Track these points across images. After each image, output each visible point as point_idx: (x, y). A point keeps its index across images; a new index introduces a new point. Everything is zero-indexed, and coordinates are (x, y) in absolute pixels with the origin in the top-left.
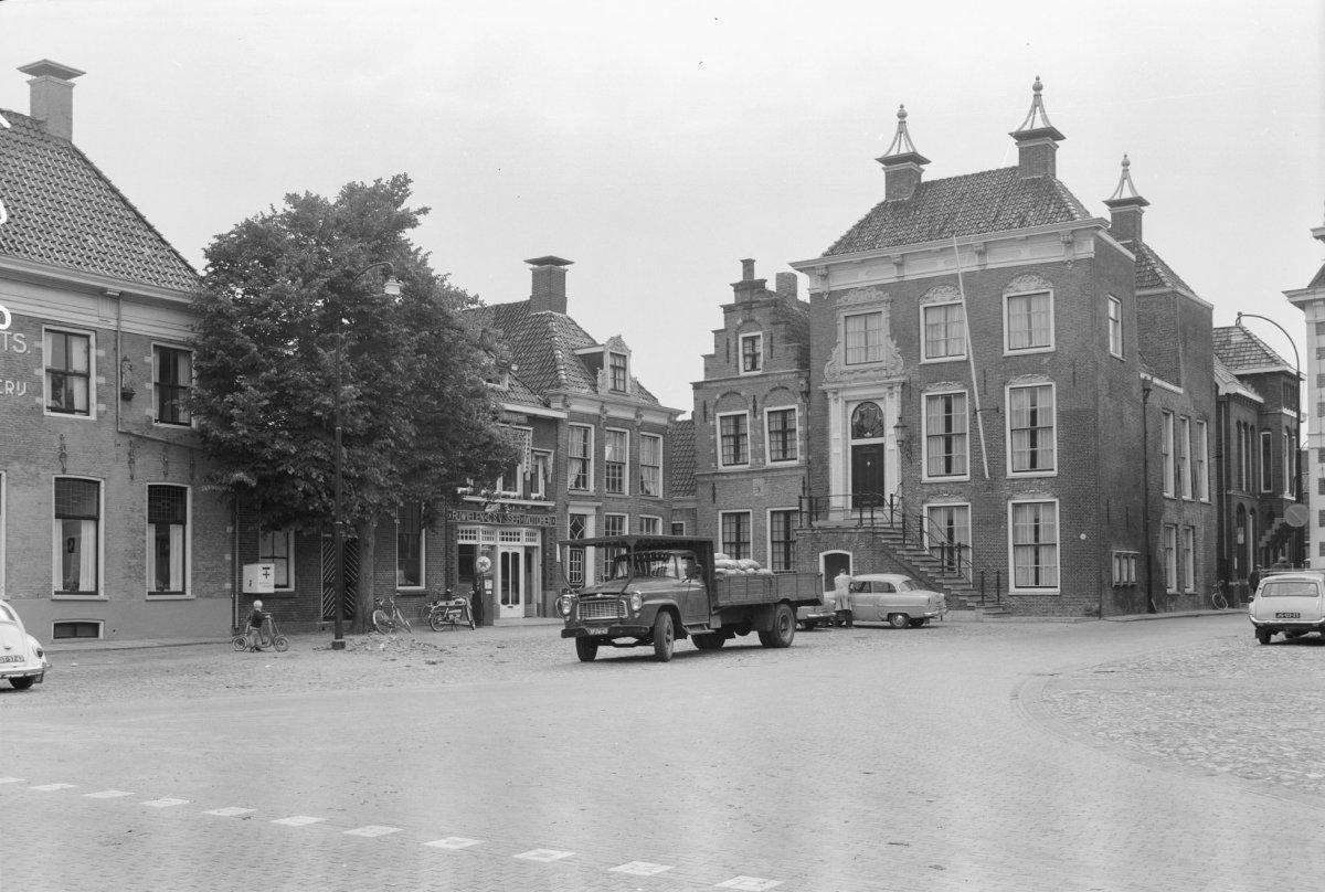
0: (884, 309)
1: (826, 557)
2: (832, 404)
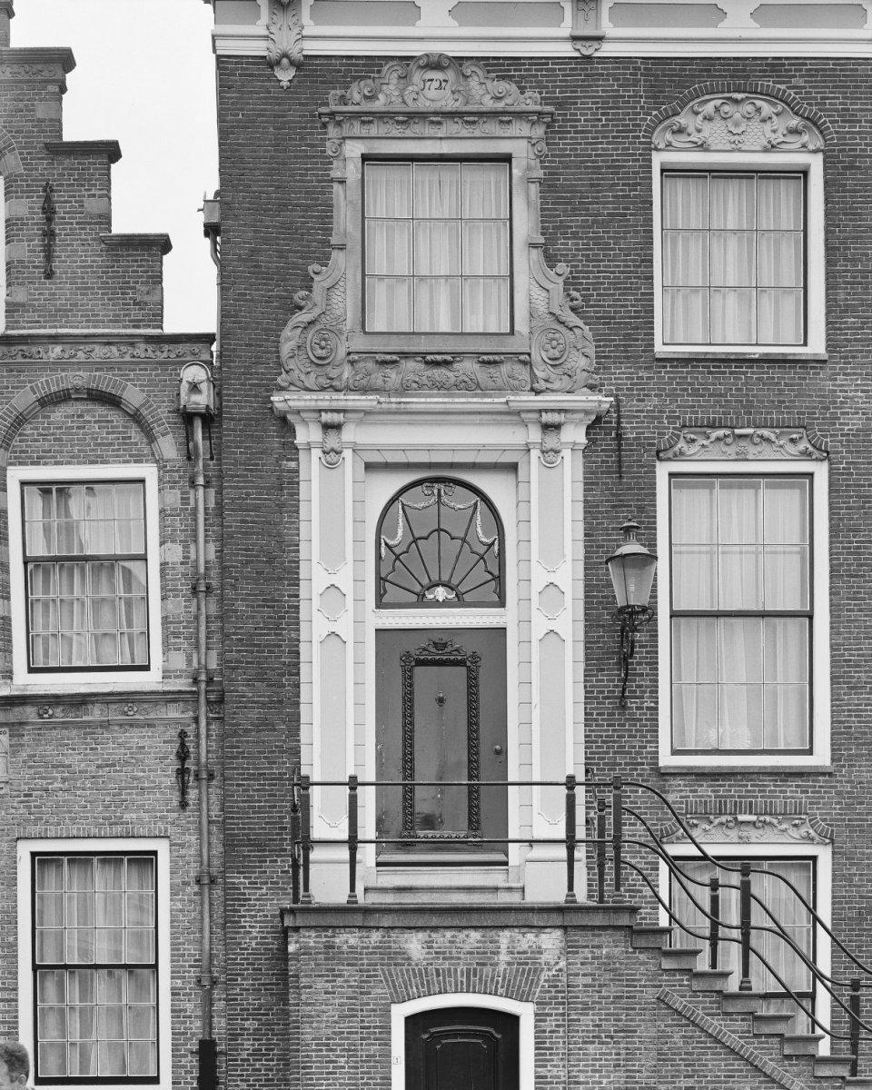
0: (520, 143)
1: (410, 1020)
2: (311, 469)
